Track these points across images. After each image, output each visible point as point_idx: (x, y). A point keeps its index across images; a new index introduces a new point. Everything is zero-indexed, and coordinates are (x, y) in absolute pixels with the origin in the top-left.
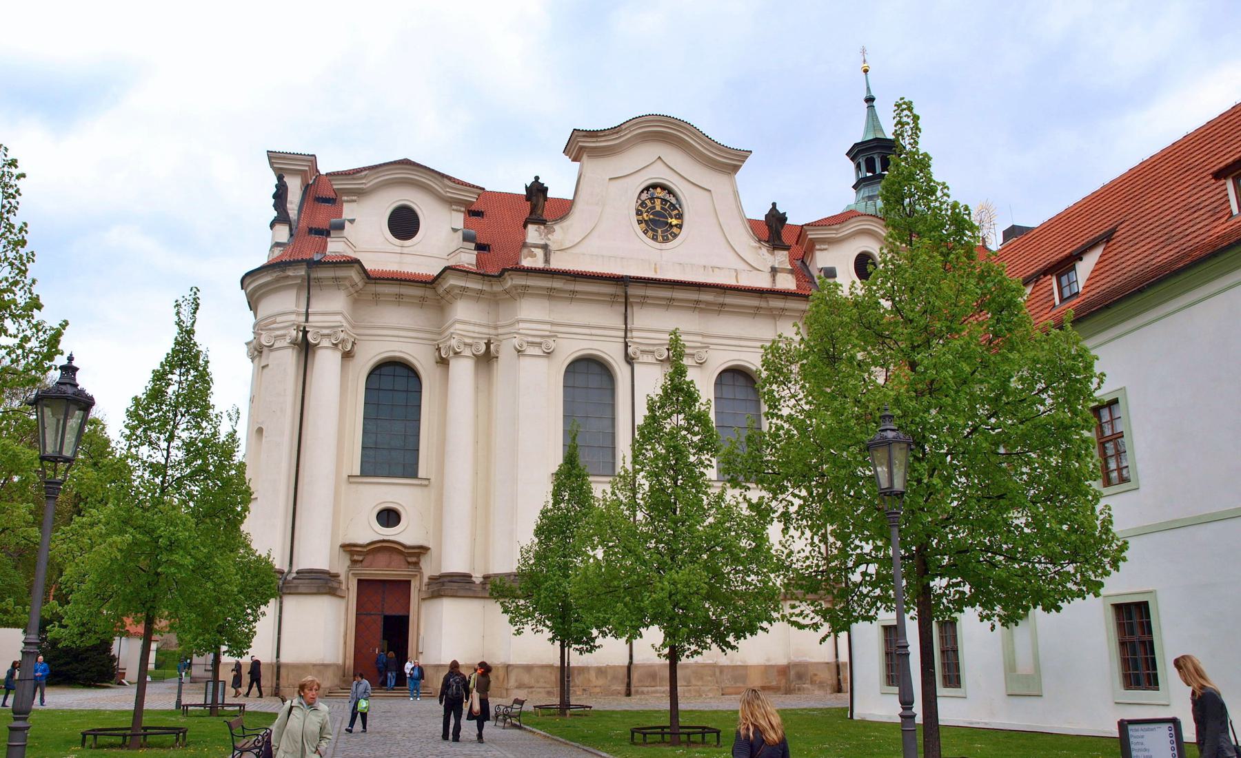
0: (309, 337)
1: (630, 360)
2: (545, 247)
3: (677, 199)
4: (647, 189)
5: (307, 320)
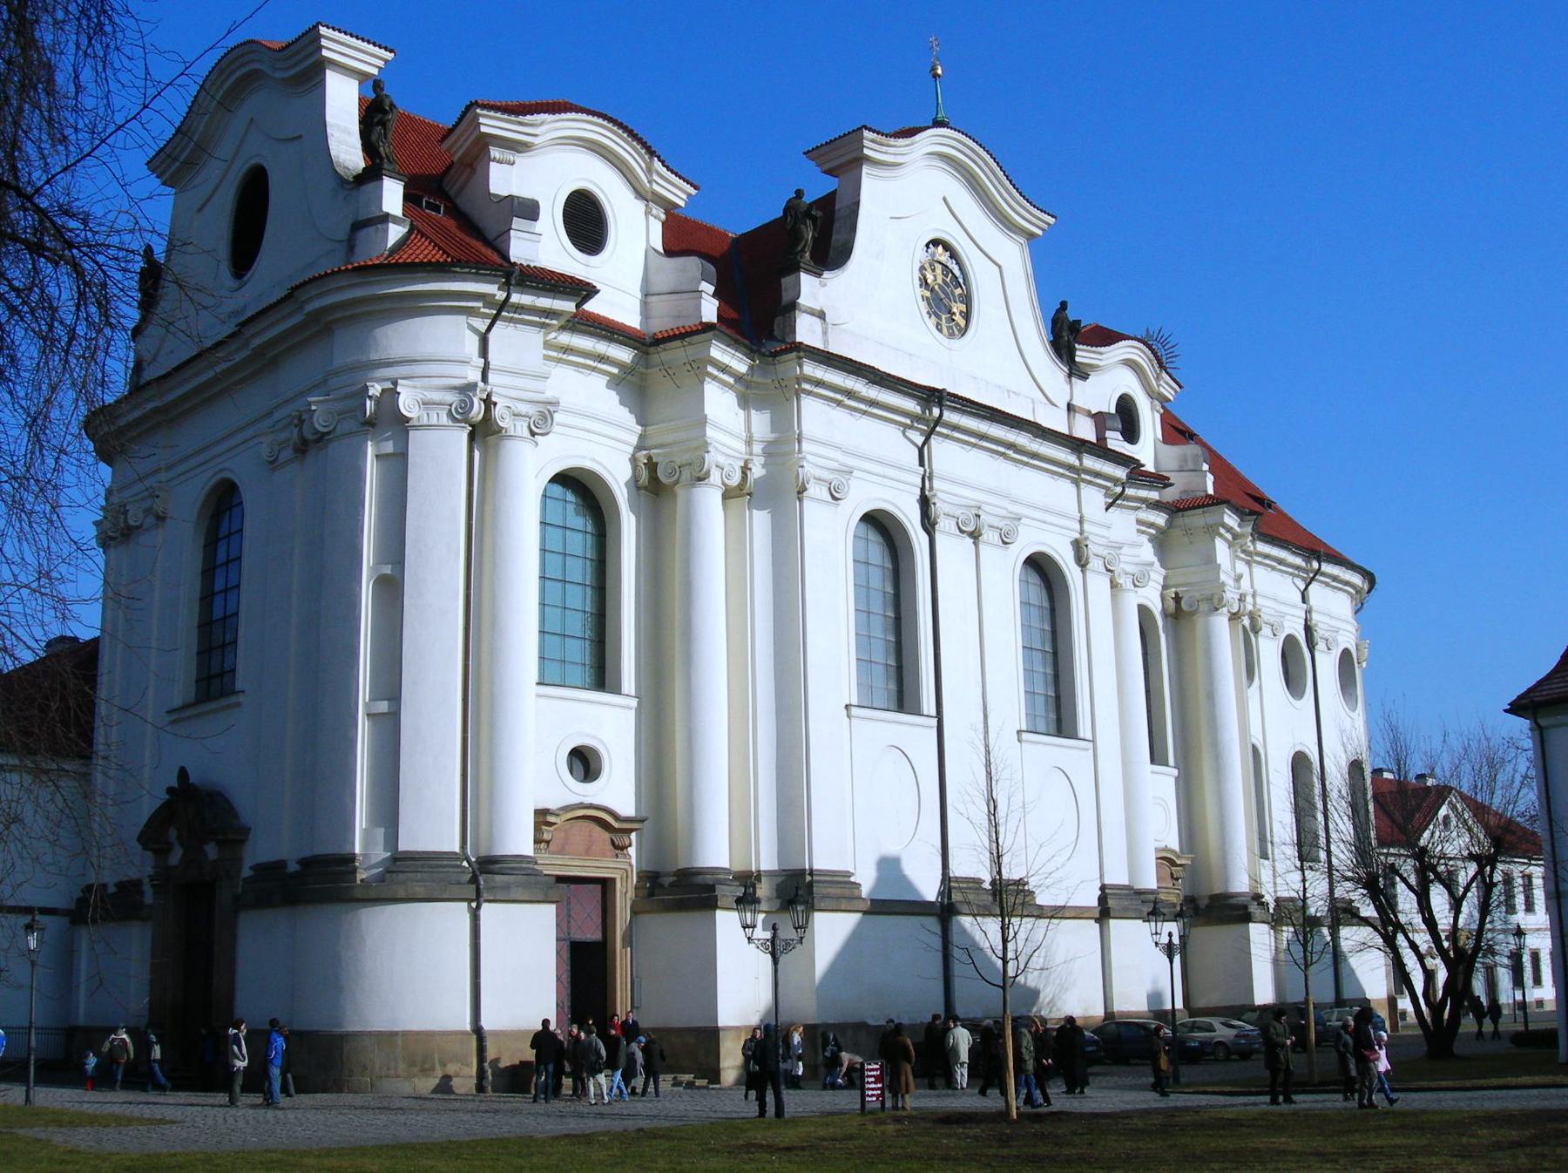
0: (498, 412)
1: (928, 524)
2: (821, 315)
3: (960, 269)
4: (927, 246)
5: (485, 378)
